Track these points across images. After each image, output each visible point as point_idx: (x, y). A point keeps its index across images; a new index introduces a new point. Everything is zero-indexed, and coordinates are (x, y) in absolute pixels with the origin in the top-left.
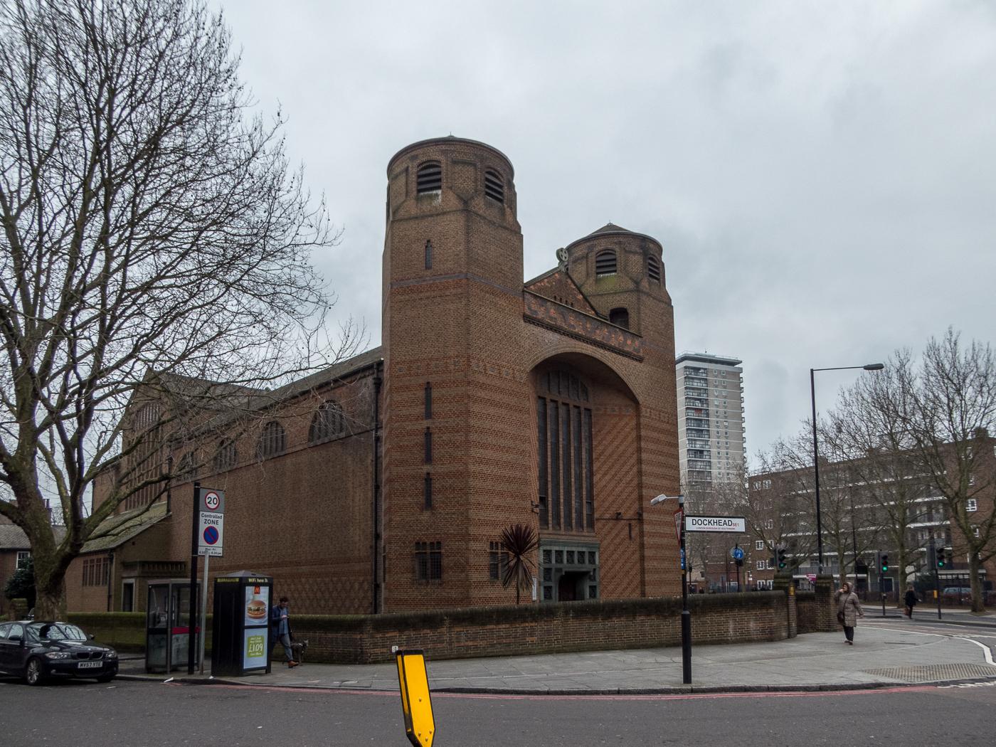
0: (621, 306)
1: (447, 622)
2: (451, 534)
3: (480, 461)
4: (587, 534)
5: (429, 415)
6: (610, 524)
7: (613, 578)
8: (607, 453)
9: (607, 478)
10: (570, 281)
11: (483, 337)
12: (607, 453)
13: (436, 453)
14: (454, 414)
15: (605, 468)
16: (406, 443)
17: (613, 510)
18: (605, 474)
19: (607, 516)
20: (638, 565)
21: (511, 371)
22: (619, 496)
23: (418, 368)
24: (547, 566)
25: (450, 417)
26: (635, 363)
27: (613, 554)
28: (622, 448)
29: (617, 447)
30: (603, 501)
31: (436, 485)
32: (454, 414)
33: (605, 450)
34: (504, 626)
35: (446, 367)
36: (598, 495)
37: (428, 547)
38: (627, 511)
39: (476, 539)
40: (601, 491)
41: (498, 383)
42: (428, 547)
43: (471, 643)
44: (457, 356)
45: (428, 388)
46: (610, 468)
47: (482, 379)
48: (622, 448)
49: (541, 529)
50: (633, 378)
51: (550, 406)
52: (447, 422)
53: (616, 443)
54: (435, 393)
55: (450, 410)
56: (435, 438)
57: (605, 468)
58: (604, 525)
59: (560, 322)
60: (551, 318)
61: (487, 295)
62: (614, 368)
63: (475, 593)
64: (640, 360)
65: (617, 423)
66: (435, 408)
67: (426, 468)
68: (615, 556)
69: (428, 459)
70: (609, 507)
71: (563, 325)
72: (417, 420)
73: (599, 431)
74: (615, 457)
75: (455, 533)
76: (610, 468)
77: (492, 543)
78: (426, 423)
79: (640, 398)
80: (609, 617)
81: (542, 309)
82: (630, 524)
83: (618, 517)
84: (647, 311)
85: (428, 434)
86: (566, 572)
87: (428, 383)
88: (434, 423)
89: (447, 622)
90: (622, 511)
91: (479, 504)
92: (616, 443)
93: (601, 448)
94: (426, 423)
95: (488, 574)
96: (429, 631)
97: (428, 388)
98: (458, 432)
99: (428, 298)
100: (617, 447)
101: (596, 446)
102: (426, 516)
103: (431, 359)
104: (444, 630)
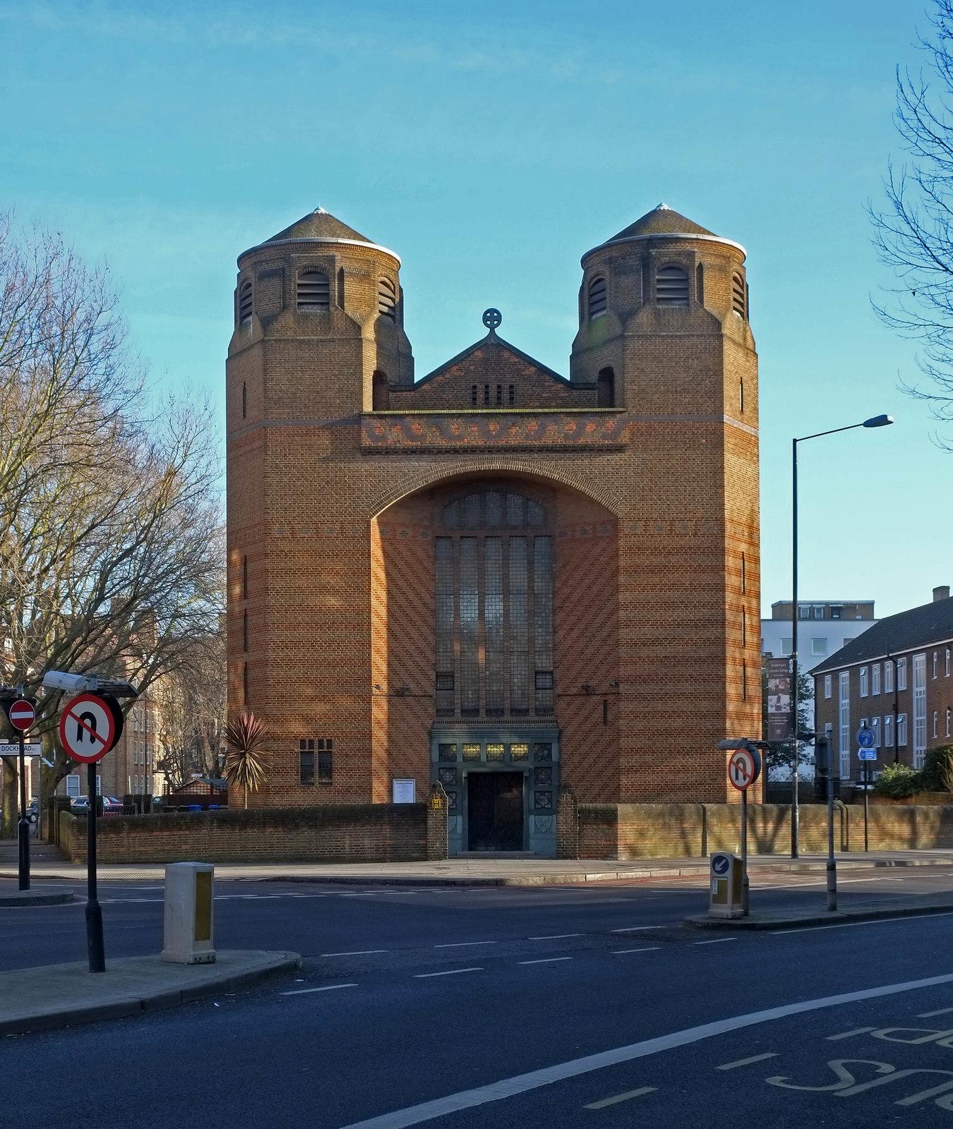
1: (126, 827)
4: (509, 719)
6: (578, 701)
7: (579, 781)
9: (574, 635)
10: (506, 354)
17: (581, 682)
19: (574, 691)
21: (337, 526)
22: (590, 660)
26: (616, 457)
27: (580, 745)
28: (595, 589)
30: (568, 669)
33: (571, 593)
38: (601, 681)
40: (565, 655)
43: (142, 849)
46: (579, 620)
48: (595, 589)
49: (437, 716)
53: (587, 581)
58: (569, 704)
60: (413, 438)
64: (620, 449)
68: (584, 749)
70: (576, 678)
73: (564, 566)
77: (303, 741)
79: (621, 510)
82: (605, 701)
83: (587, 691)
89: (126, 827)
90: (592, 683)
91: (282, 697)
92: (587, 581)
93: (566, 591)
96: (113, 835)
104: (124, 834)
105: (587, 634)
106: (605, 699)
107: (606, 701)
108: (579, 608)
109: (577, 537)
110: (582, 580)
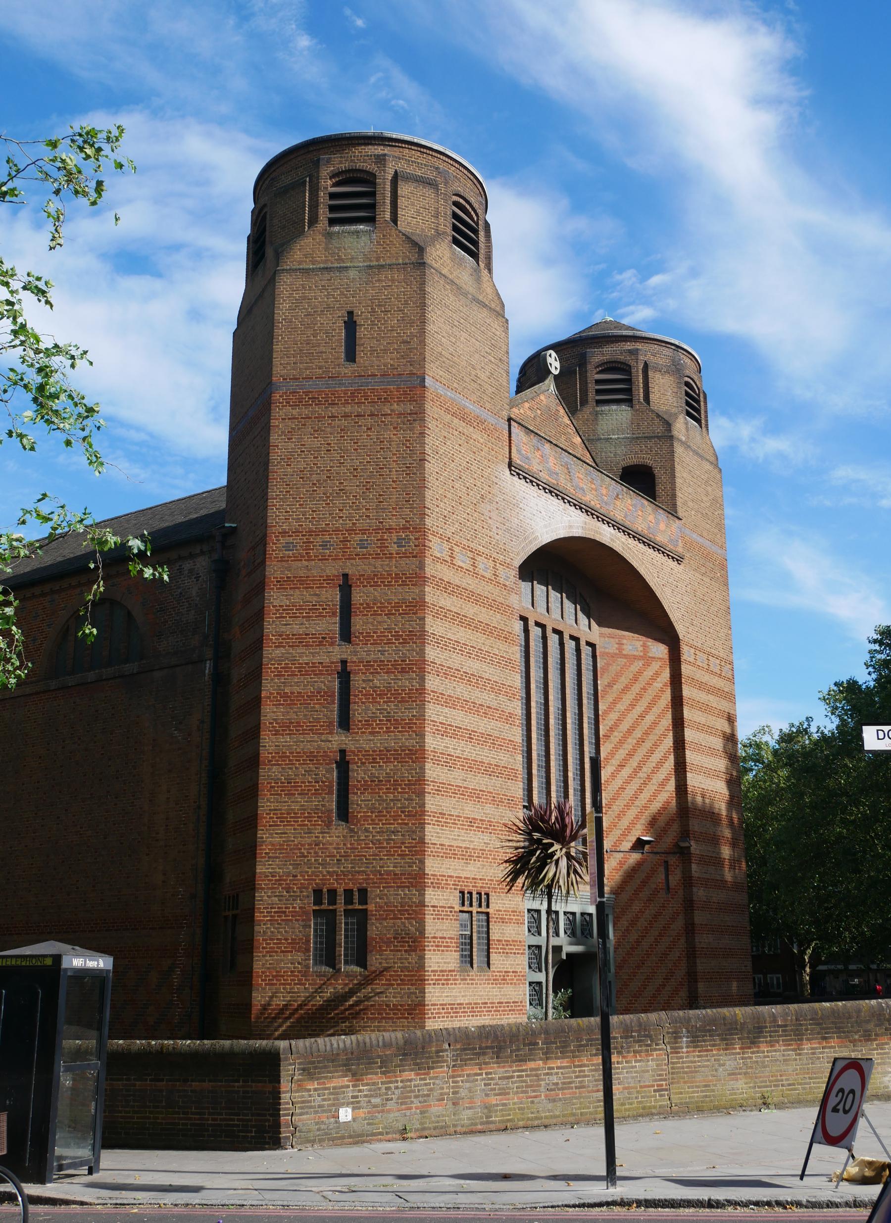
0: (641, 461)
1: (448, 1055)
2: (388, 873)
3: (447, 730)
5: (346, 635)
8: (625, 726)
9: (626, 772)
11: (449, 495)
12: (625, 726)
13: (358, 712)
14: (397, 637)
15: (621, 754)
16: (296, 689)
18: (622, 766)
20: (683, 940)
23: (324, 546)
24: (534, 940)
25: (389, 643)
26: (673, 564)
28: (650, 718)
29: (642, 716)
31: (358, 774)
32: (397, 637)
34: (559, 1063)
35: (383, 547)
36: (609, 806)
37: (341, 899)
39: (437, 886)
41: (469, 582)
42: (341, 899)
44: (405, 528)
45: (346, 586)
46: (630, 755)
47: (447, 574)
48: (650, 718)
50: (668, 591)
51: (535, 632)
52: (382, 652)
53: (639, 709)
54: (358, 596)
55: (389, 630)
56: (357, 682)
57: (621, 754)
59: (563, 483)
61: (456, 421)
62: (642, 571)
63: (434, 995)
64: (678, 560)
65: (640, 673)
66: (358, 623)
67: (338, 740)
69: (345, 722)
71: (569, 486)
72: (321, 644)
74: (638, 734)
75: (398, 870)
76: (630, 755)
78: (338, 652)
80: (754, 1042)
81: (538, 454)
84: (685, 475)
85: (344, 675)
86: (567, 954)
87: (345, 576)
88: (355, 653)
89: (448, 1055)
92: (639, 709)
94: (338, 652)
95: (457, 955)
96: (412, 1075)
97: (346, 586)
98: (403, 671)
99: (346, 416)
100: (642, 716)
101: (606, 712)
102: (337, 833)
103: (351, 531)
104: (442, 1071)
105: (641, 775)
106: (666, 859)
107: (667, 862)
108: (629, 740)
109: (624, 652)
110: (632, 705)
